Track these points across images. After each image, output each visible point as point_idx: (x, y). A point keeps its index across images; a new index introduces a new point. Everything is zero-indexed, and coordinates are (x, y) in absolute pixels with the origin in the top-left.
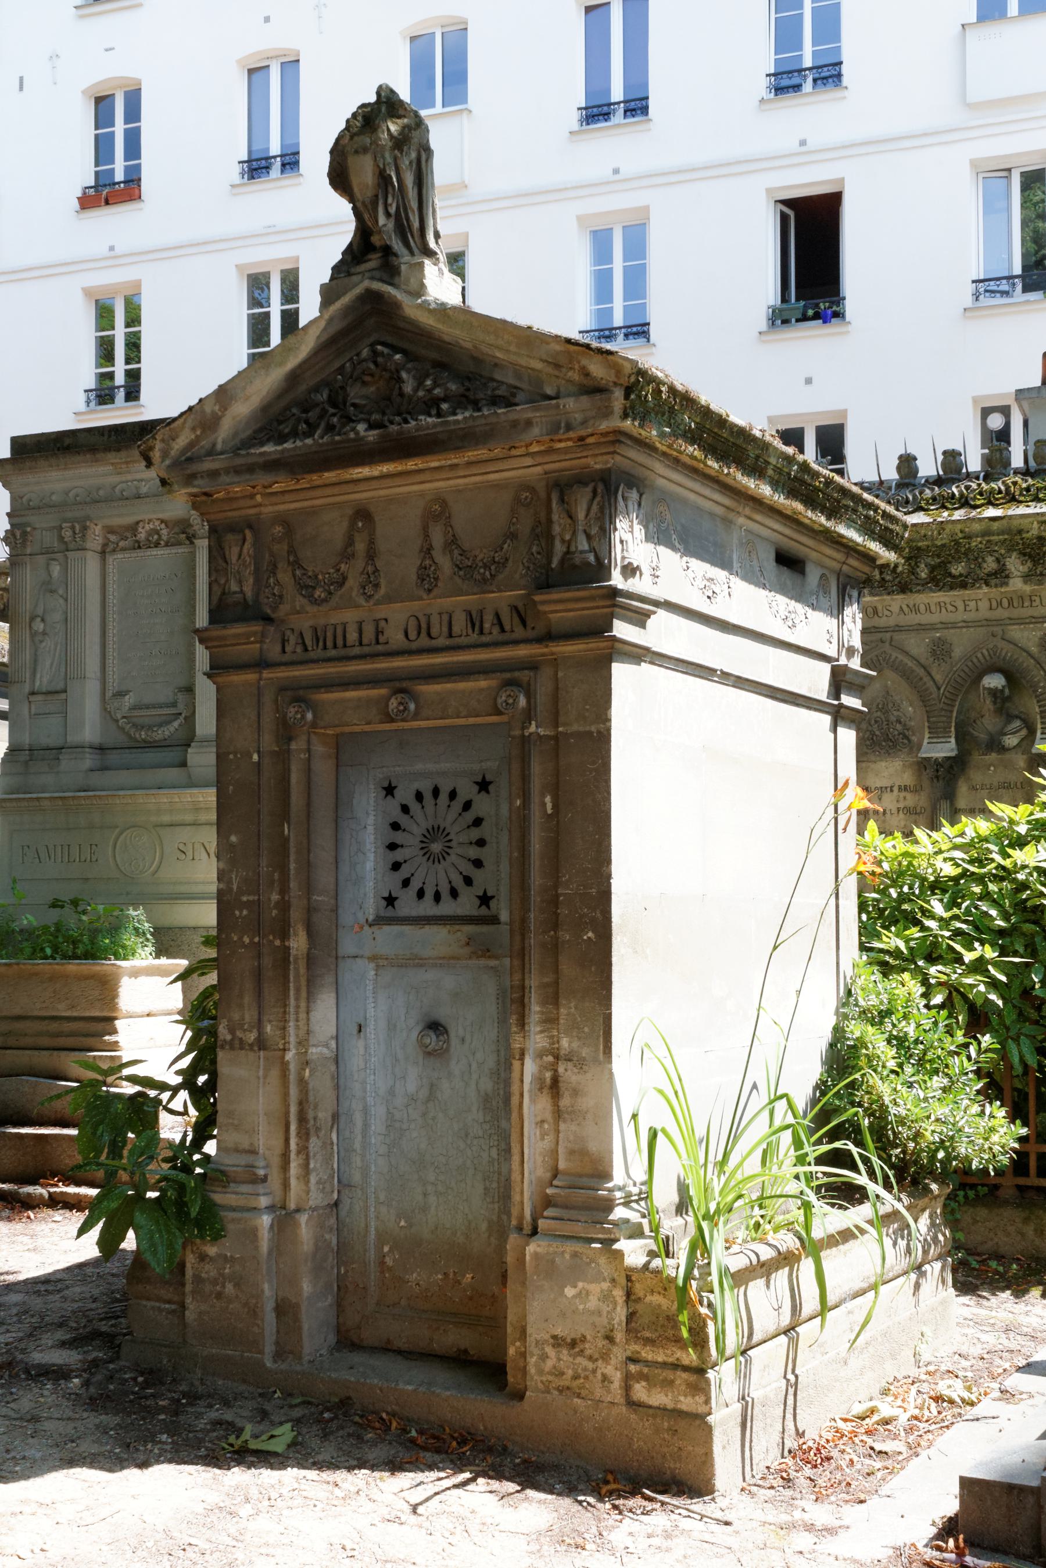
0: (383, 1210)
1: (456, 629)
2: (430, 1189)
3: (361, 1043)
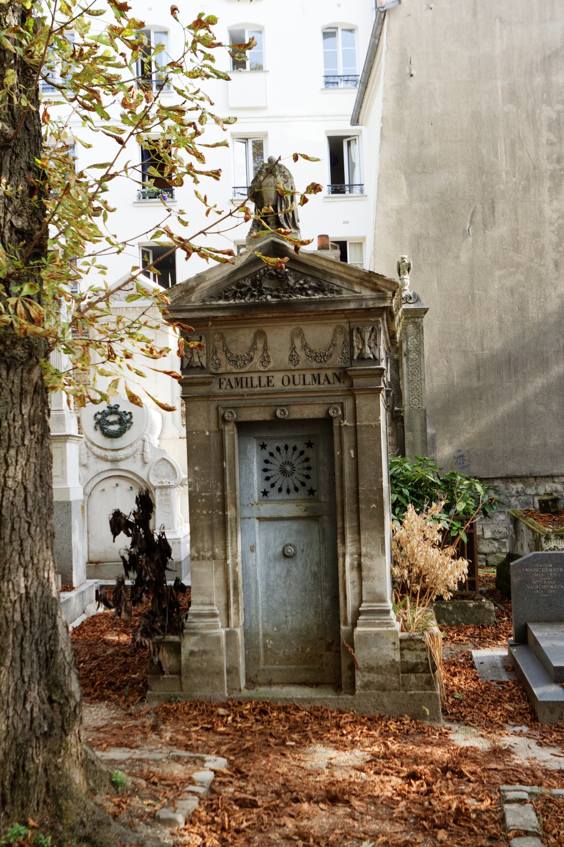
0: (266, 624)
1: (307, 382)
2: (288, 614)
3: (254, 554)
